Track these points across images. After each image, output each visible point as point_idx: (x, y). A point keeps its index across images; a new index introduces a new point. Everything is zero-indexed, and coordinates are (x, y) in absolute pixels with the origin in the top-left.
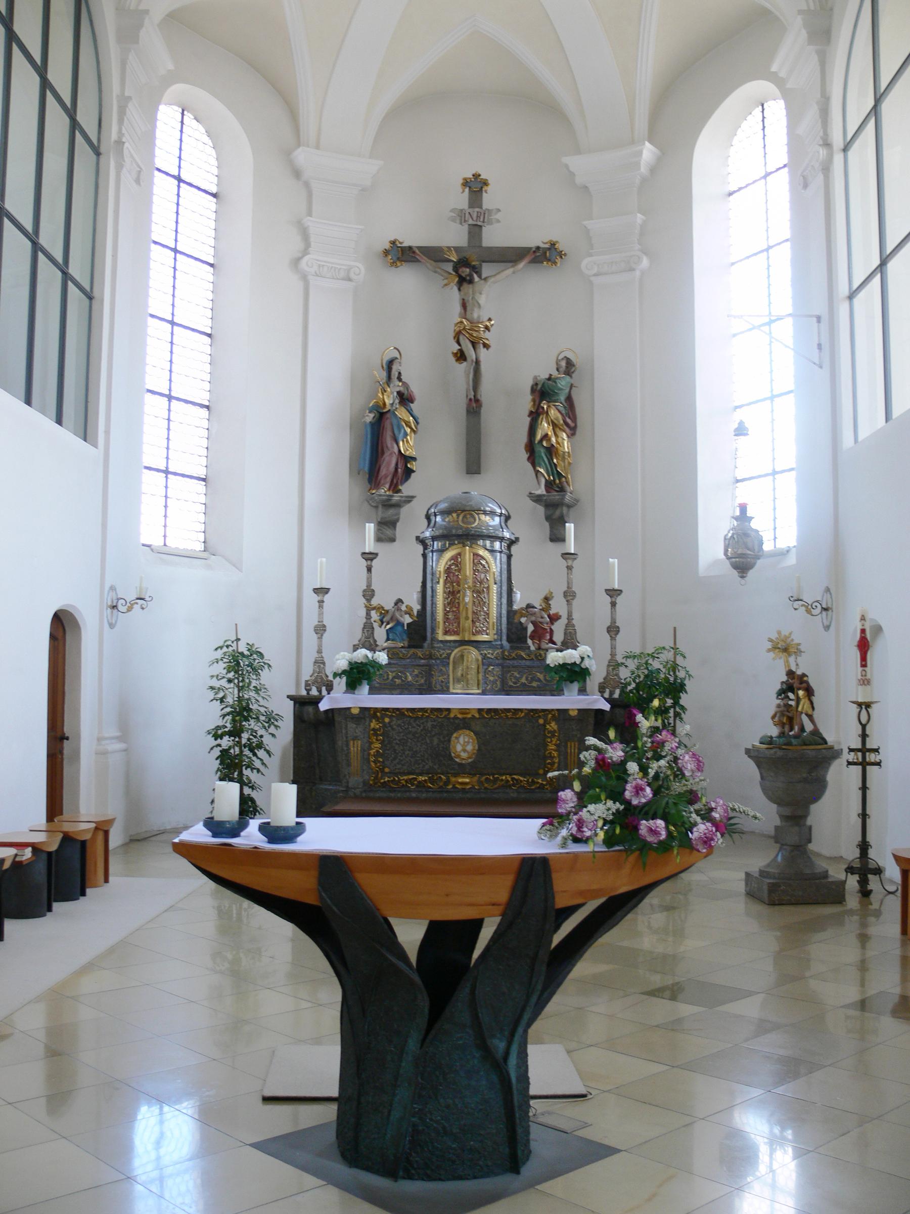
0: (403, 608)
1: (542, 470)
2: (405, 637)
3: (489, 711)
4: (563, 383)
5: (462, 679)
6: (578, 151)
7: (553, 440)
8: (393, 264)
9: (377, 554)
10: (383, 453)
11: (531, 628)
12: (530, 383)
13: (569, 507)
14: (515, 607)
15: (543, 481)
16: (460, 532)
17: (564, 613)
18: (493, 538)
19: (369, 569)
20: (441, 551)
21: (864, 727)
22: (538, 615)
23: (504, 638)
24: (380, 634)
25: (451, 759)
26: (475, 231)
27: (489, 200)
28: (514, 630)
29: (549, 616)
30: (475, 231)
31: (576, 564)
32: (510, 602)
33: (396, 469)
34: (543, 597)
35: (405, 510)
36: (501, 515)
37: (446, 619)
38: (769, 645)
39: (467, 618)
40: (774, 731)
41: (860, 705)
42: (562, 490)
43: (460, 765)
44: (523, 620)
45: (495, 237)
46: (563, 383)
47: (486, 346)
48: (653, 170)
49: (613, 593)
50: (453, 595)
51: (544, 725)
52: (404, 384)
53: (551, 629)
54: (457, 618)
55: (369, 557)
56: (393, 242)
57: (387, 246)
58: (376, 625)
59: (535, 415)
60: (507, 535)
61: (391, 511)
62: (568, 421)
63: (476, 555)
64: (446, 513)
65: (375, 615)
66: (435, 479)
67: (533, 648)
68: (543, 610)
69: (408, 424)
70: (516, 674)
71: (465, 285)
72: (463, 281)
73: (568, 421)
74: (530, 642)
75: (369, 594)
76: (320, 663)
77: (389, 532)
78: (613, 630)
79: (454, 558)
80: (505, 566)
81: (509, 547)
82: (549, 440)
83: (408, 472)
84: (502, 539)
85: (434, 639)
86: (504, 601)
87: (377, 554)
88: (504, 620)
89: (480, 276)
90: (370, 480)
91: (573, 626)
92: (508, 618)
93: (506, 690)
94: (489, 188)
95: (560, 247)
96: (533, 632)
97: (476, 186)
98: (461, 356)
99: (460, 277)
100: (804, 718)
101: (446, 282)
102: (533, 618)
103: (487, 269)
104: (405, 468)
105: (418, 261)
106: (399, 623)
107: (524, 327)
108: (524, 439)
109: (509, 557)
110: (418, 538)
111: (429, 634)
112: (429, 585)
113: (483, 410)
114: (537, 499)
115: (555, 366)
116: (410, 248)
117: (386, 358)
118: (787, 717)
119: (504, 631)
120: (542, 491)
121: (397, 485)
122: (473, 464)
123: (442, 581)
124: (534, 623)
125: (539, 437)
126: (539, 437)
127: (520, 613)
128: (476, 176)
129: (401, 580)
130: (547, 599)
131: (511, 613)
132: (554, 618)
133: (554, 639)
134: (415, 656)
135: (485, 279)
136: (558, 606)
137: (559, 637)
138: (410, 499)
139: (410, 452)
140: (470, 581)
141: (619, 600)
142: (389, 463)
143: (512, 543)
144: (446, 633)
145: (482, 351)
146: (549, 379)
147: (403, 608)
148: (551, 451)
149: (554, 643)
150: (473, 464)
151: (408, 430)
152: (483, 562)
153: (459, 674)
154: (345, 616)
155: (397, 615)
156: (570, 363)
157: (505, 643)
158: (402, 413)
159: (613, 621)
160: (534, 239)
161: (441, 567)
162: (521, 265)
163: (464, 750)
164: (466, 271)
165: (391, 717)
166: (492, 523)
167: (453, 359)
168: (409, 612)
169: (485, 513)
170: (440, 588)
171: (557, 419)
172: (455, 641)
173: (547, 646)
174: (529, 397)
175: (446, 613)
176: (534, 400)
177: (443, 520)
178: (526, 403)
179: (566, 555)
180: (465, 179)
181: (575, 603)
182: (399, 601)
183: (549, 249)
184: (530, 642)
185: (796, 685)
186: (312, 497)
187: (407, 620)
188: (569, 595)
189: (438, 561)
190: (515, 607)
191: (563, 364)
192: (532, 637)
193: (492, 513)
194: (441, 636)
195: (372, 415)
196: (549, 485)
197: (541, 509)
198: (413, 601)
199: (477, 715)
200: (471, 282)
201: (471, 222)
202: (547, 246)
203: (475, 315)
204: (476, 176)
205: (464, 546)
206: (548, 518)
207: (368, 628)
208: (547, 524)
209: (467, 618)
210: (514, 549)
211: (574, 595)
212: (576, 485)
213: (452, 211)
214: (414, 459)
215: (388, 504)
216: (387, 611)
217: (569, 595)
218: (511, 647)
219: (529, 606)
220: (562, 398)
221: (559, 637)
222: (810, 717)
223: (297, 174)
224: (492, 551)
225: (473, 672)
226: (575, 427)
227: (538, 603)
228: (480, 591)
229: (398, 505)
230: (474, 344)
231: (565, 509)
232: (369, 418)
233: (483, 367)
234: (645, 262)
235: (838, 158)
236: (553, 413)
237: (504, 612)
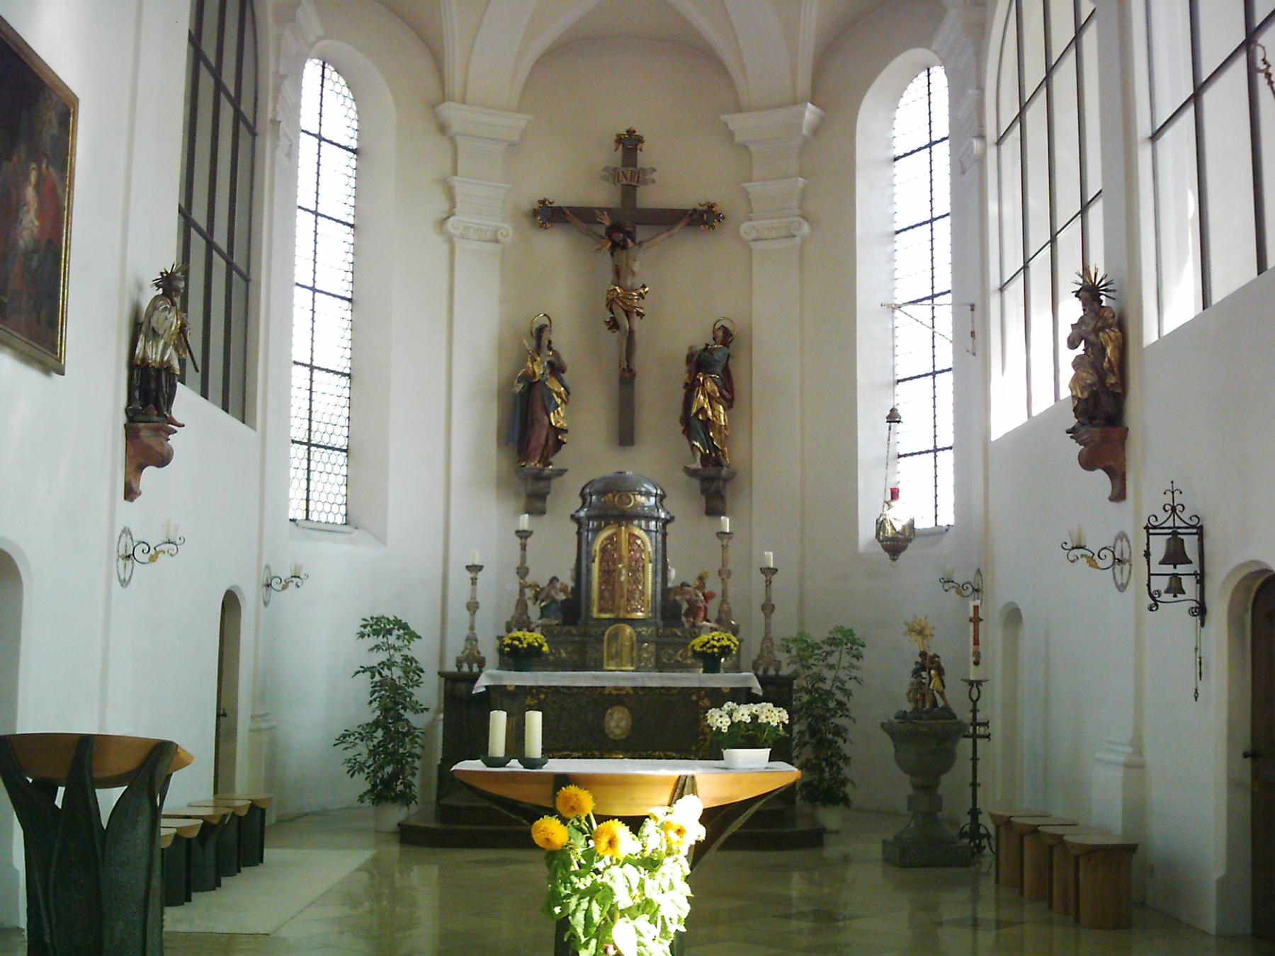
0: (558, 586)
1: (697, 444)
2: (559, 614)
3: (643, 688)
4: (720, 354)
5: (616, 657)
6: (739, 109)
7: (710, 413)
8: (542, 226)
9: (531, 532)
10: (533, 424)
11: (685, 606)
12: (685, 352)
13: (726, 480)
14: (670, 585)
15: (699, 454)
16: (615, 512)
18: (649, 518)
19: (524, 547)
20: (597, 531)
21: (975, 703)
23: (659, 615)
24: (534, 611)
25: (606, 736)
26: (629, 192)
27: (643, 159)
30: (629, 192)
31: (731, 543)
32: (665, 579)
33: (547, 442)
34: (697, 574)
35: (555, 483)
36: (656, 495)
37: (601, 597)
38: (906, 628)
39: (622, 597)
40: (908, 707)
41: (971, 683)
42: (718, 464)
43: (614, 741)
44: (678, 598)
45: (649, 198)
46: (719, 356)
47: (641, 315)
48: (816, 130)
49: (769, 572)
50: (609, 574)
51: (697, 702)
52: (556, 354)
54: (612, 596)
55: (523, 535)
56: (543, 202)
57: (537, 206)
58: (530, 603)
59: (691, 388)
60: (663, 515)
61: (542, 484)
62: (725, 393)
63: (632, 535)
64: (601, 493)
65: (529, 593)
66: (587, 453)
67: (687, 626)
68: (698, 588)
69: (559, 395)
70: (671, 652)
71: (618, 251)
72: (617, 247)
73: (725, 393)
74: (684, 619)
75: (522, 571)
76: (471, 639)
77: (538, 504)
78: (768, 608)
79: (610, 538)
80: (660, 545)
81: (664, 526)
82: (706, 412)
83: (559, 444)
84: (658, 519)
85: (588, 617)
86: (659, 579)
87: (531, 532)
88: (659, 597)
89: (633, 241)
90: (520, 452)
92: (663, 595)
93: (660, 667)
94: (644, 146)
95: (717, 209)
97: (629, 143)
98: (614, 325)
99: (613, 241)
100: (938, 696)
101: (598, 246)
103: (641, 233)
104: (556, 439)
105: (568, 222)
106: (554, 601)
107: (683, 294)
108: (679, 411)
109: (665, 535)
110: (572, 516)
111: (583, 612)
112: (584, 563)
113: (637, 380)
114: (692, 473)
115: (711, 336)
116: (560, 208)
117: (536, 326)
118: (919, 691)
119: (659, 609)
120: (697, 465)
121: (547, 457)
122: (626, 436)
123: (597, 560)
124: (689, 601)
125: (694, 410)
126: (694, 410)
128: (631, 132)
129: (555, 558)
130: (701, 579)
131: (666, 591)
132: (707, 597)
133: (709, 617)
134: (570, 633)
135: (640, 244)
136: (713, 585)
137: (713, 613)
138: (561, 472)
139: (562, 424)
140: (626, 560)
141: (775, 578)
142: (539, 437)
143: (666, 522)
144: (601, 610)
145: (636, 319)
146: (706, 349)
147: (558, 586)
148: (708, 424)
150: (626, 436)
151: (559, 401)
152: (639, 542)
153: (614, 651)
154: (497, 594)
155: (553, 593)
156: (726, 331)
157: (660, 622)
158: (553, 385)
159: (768, 599)
160: (689, 198)
161: (597, 546)
162: (676, 230)
163: (618, 727)
164: (619, 237)
165: (546, 694)
166: (647, 504)
167: (605, 327)
168: (564, 590)
169: (641, 493)
170: (596, 567)
171: (714, 391)
172: (609, 619)
174: (684, 368)
175: (601, 591)
176: (689, 372)
177: (599, 500)
178: (681, 373)
179: (721, 534)
180: (618, 135)
182: (554, 580)
183: (706, 212)
184: (684, 619)
185: (928, 664)
186: (460, 468)
187: (562, 597)
188: (724, 573)
189: (594, 539)
190: (670, 585)
191: (720, 334)
192: (687, 615)
193: (648, 494)
194: (595, 614)
195: (521, 386)
196: (705, 459)
197: (696, 483)
198: (567, 579)
199: (631, 692)
200: (624, 247)
201: (624, 182)
202: (705, 208)
203: (629, 283)
204: (631, 132)
205: (620, 526)
206: (703, 491)
207: (522, 605)
208: (703, 499)
209: (622, 597)
210: (669, 527)
211: (729, 573)
212: (734, 456)
213: (606, 169)
214: (565, 431)
215: (538, 477)
216: (542, 589)
217: (724, 573)
218: (666, 625)
219: (683, 585)
220: (719, 370)
221: (713, 613)
222: (942, 694)
223: (442, 128)
224: (648, 531)
225: (627, 649)
226: (733, 399)
227: (693, 581)
228: (636, 569)
229: (548, 478)
230: (628, 314)
231: (721, 483)
232: (519, 388)
233: (637, 336)
234: (806, 228)
235: (992, 152)
236: (709, 384)
237: (659, 590)
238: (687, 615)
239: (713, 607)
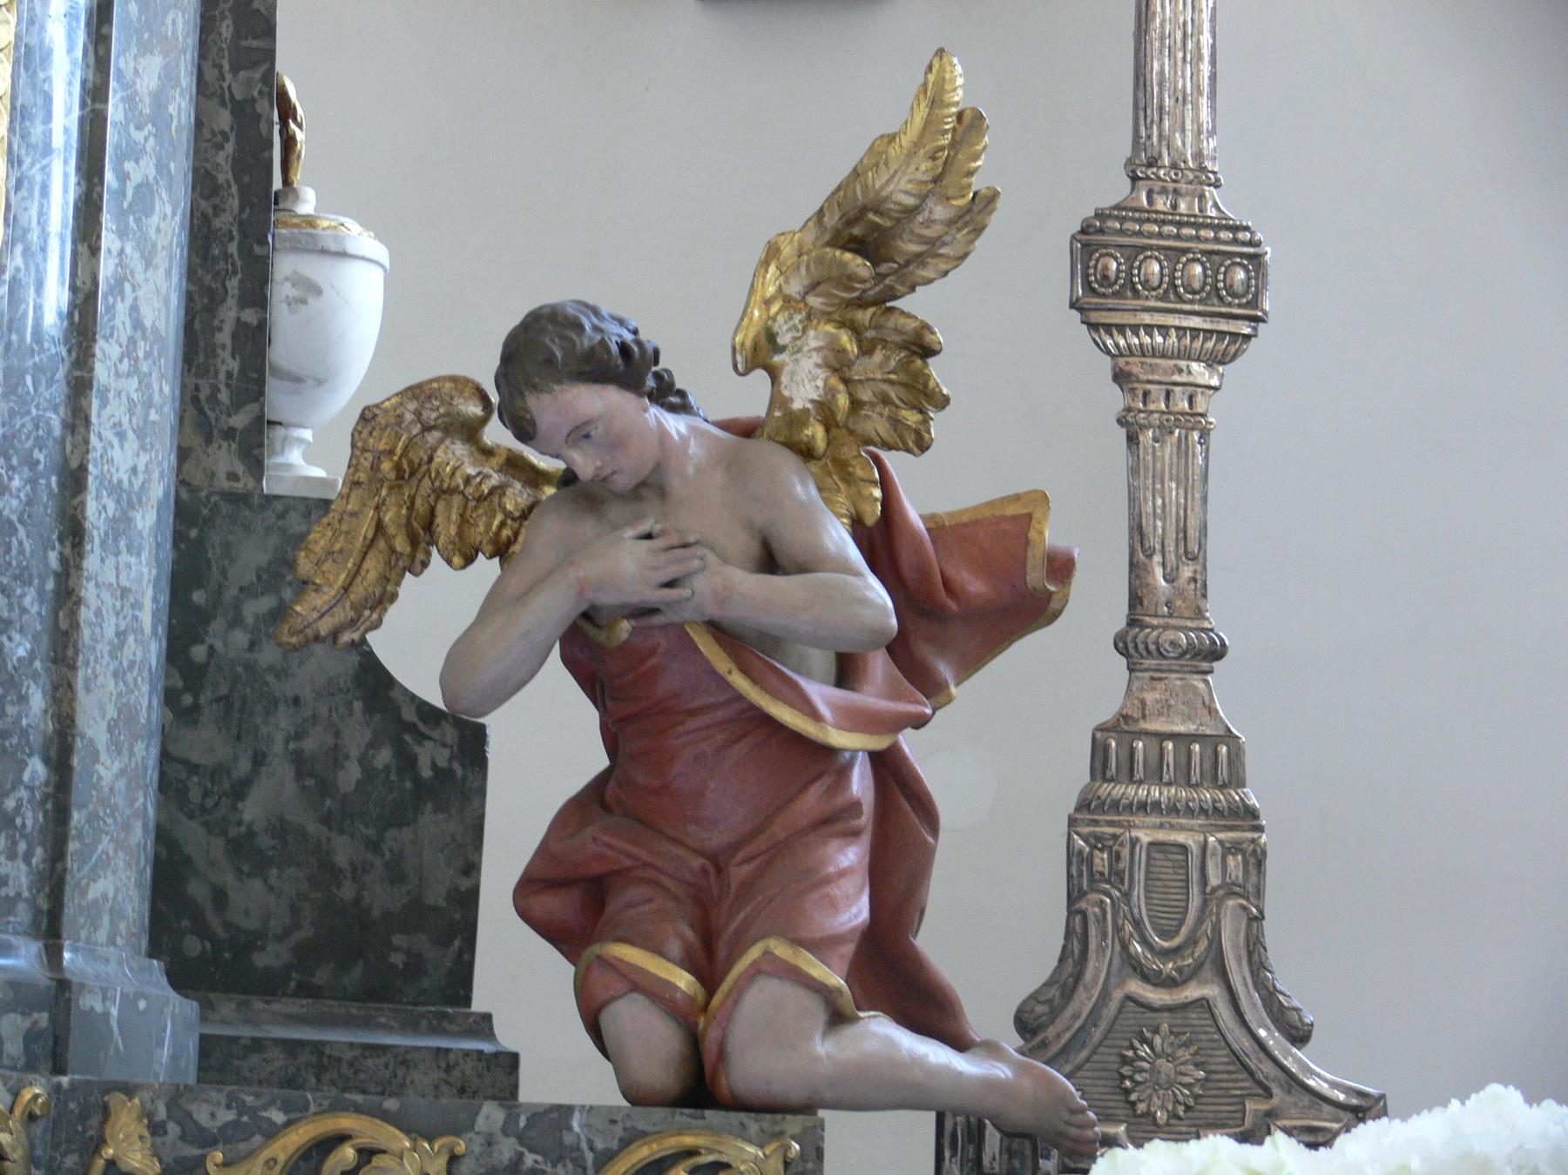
11: (544, 751)
17: (1086, 528)
22: (709, 512)
23: (113, 884)
28: (272, 796)
29: (881, 540)
34: (797, 198)
44: (424, 629)
53: (891, 770)
68: (780, 430)
91: (1219, 758)
92: (184, 624)
96: (593, 801)
102: (623, 564)
124: (601, 654)
127: (414, 488)
130: (870, 249)
132: (964, 597)
133: (937, 941)
137: (992, 922)
149: (928, 1009)
157: (112, 964)
173: (828, 1051)
181: (1242, 400)
184: (520, 982)
192: (575, 898)
218: (217, 1060)
219: (549, 350)
227: (698, 285)
238: (575, 898)
239: (1002, 756)
